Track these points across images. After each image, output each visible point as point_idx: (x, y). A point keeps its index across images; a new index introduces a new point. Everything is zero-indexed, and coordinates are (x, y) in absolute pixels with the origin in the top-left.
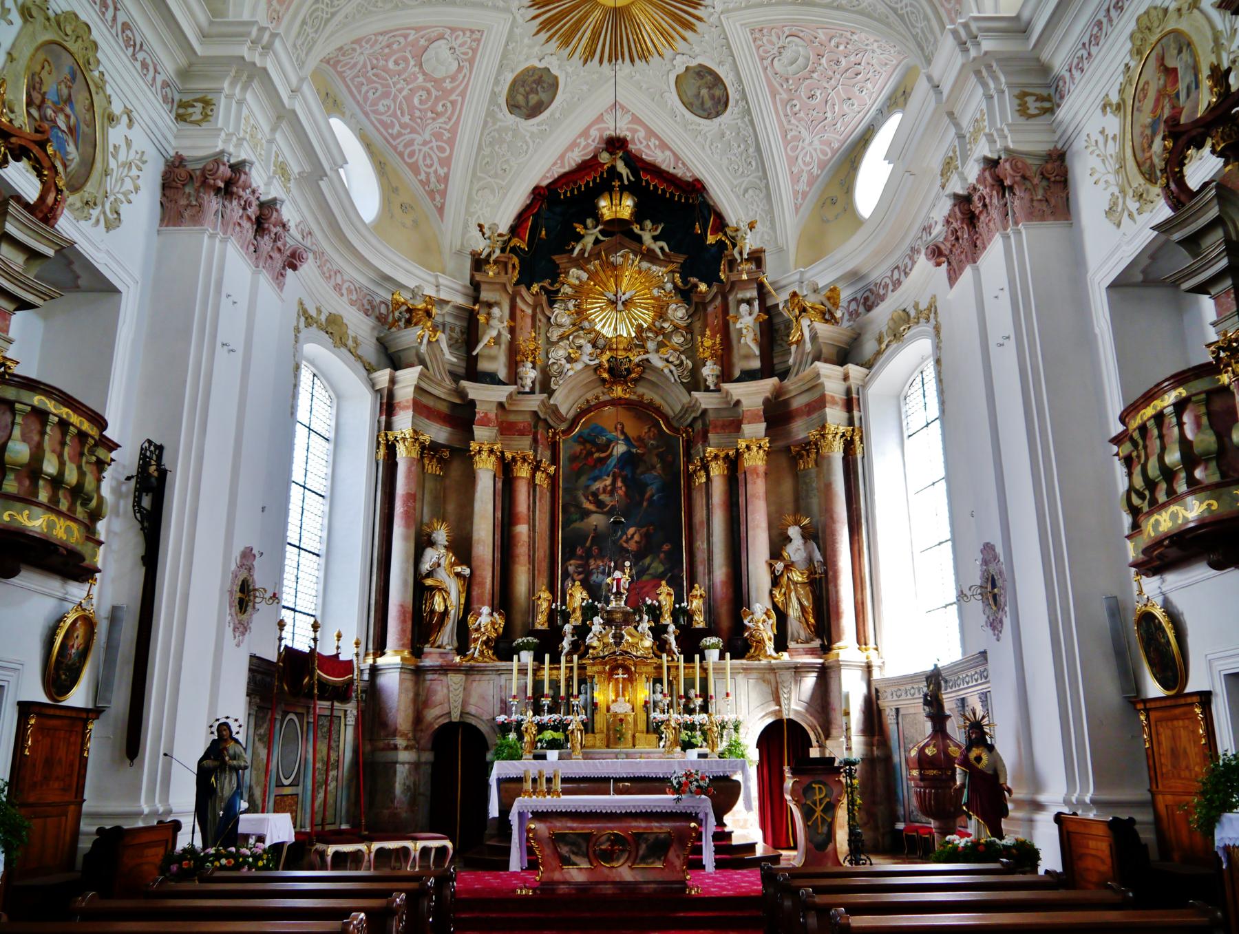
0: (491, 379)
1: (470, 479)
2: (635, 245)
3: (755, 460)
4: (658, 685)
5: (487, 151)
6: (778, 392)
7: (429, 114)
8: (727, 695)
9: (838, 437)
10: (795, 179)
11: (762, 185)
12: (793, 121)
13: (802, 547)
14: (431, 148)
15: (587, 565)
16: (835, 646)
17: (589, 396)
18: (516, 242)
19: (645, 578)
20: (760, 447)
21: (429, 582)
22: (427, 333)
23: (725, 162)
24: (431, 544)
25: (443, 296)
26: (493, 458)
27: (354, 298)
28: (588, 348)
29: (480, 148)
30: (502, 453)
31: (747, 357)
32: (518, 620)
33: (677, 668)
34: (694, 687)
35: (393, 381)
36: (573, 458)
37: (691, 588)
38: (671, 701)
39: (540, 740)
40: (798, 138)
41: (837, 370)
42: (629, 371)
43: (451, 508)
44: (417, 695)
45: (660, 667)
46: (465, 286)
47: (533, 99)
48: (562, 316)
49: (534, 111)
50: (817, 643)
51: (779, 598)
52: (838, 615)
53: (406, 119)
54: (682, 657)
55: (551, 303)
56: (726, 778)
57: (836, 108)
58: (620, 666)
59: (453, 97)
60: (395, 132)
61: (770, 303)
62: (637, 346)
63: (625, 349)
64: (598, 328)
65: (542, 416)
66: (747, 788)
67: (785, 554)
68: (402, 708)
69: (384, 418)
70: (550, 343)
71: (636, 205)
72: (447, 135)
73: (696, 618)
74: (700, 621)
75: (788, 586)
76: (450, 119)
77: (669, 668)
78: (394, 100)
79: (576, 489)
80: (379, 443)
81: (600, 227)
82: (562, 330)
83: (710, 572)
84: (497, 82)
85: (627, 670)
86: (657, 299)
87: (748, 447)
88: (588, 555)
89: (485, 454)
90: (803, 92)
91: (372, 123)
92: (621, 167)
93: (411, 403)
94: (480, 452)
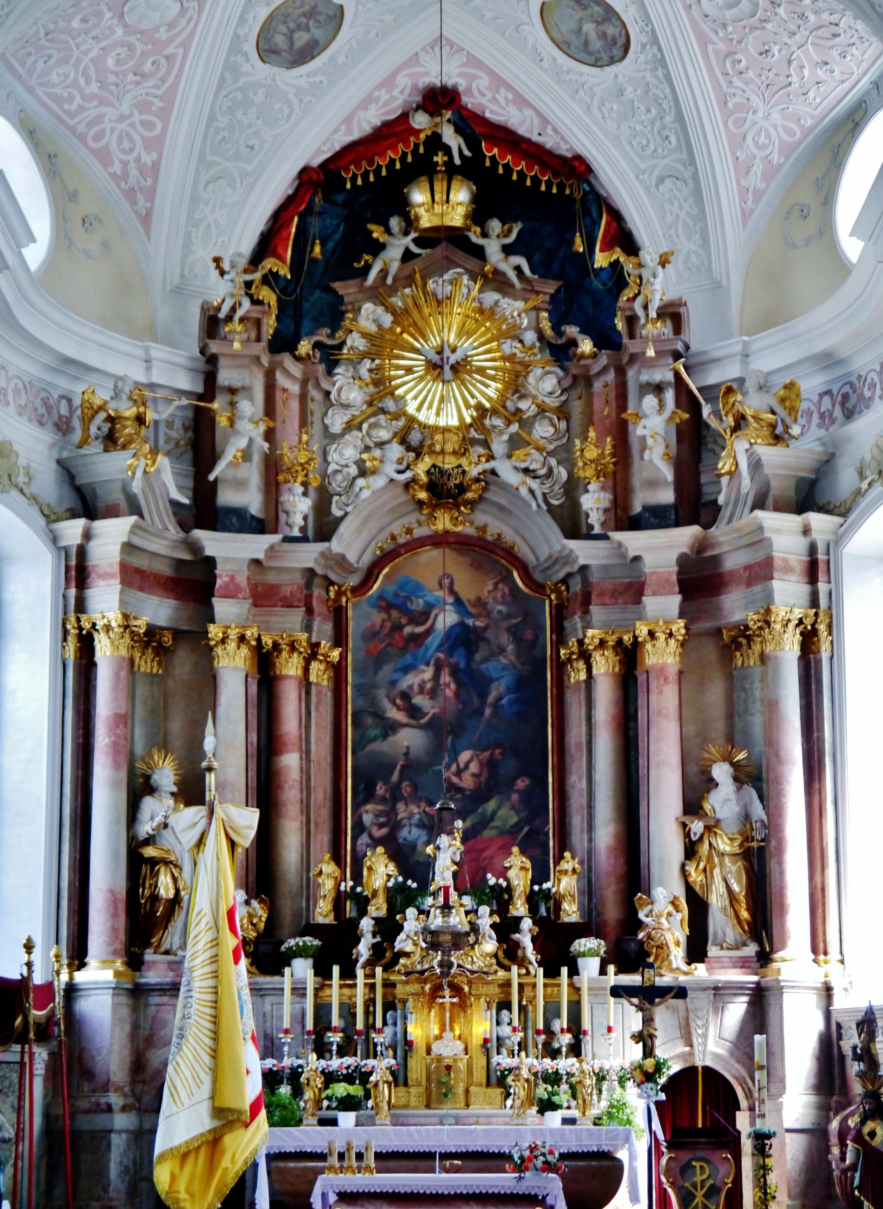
1: (208, 682)
2: (473, 263)
3: (662, 656)
4: (505, 1012)
5: (223, 121)
6: (701, 546)
7: (131, 77)
8: (610, 1029)
9: (791, 626)
10: (743, 169)
11: (688, 174)
12: (737, 82)
13: (733, 797)
14: (132, 125)
15: (393, 811)
16: (777, 956)
17: (396, 528)
19: (487, 833)
20: (671, 635)
21: (149, 852)
22: (143, 462)
24: (149, 789)
25: (156, 379)
26: (245, 651)
27: (23, 402)
28: (396, 450)
29: (212, 118)
30: (259, 639)
31: (653, 484)
32: (287, 907)
33: (534, 986)
34: (558, 1016)
35: (87, 535)
36: (371, 635)
37: (559, 858)
38: (526, 1037)
39: (329, 1098)
40: (746, 107)
41: (793, 521)
42: (462, 488)
43: (176, 726)
44: (136, 1027)
45: (507, 984)
46: (192, 359)
47: (301, 39)
48: (349, 389)
49: (304, 55)
50: (751, 949)
51: (696, 877)
53: (94, 88)
54: (541, 971)
56: (606, 1156)
57: (806, 72)
58: (448, 989)
59: (170, 50)
60: (74, 106)
62: (474, 442)
63: (454, 453)
64: (411, 409)
65: (319, 571)
66: (633, 1170)
67: (707, 807)
68: (116, 1048)
69: (72, 592)
70: (331, 437)
71: (476, 199)
72: (158, 103)
73: (565, 906)
74: (571, 913)
75: (710, 858)
76: (163, 80)
77: (521, 986)
78: (76, 66)
79: (375, 687)
80: (65, 632)
81: (413, 235)
83: (591, 828)
84: (242, 21)
85: (456, 990)
86: (511, 358)
87: (652, 634)
88: (395, 796)
89: (232, 646)
90: (752, 44)
91: (39, 100)
92: (451, 138)
93: (116, 568)
94: (223, 641)
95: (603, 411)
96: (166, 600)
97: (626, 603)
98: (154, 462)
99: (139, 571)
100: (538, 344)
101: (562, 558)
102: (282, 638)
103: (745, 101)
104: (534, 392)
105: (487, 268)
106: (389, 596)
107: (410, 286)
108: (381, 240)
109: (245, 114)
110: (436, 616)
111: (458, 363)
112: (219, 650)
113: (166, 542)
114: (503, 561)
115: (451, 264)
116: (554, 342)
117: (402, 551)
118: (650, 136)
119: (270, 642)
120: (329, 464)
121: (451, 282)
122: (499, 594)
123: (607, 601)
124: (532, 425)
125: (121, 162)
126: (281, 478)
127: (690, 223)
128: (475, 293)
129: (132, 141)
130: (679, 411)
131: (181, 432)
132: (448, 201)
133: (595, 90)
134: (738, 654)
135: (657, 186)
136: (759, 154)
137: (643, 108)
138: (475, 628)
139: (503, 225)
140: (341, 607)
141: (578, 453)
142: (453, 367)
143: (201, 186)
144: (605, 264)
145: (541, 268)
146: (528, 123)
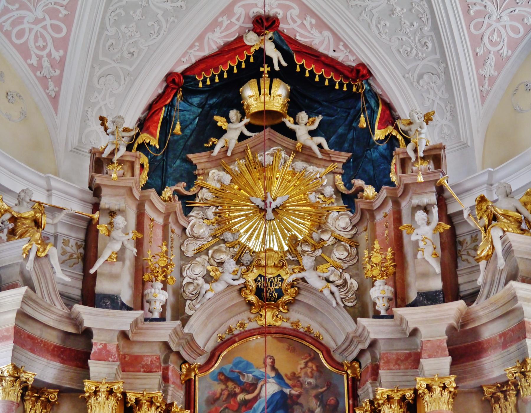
0: (113, 302)
2: (288, 142)
5: (111, 31)
6: (465, 320)
10: (480, 61)
11: (440, 69)
14: (44, 27)
17: (233, 323)
18: (144, 137)
20: (444, 388)
22: (35, 247)
25: (55, 202)
26: (112, 401)
28: (231, 265)
29: (103, 28)
30: (124, 394)
31: (425, 275)
36: (213, 400)
40: (484, 13)
42: (281, 293)
46: (82, 191)
48: (200, 225)
55: (187, 210)
61: (452, 209)
62: (290, 262)
63: (275, 266)
64: (243, 240)
65: (174, 348)
71: (291, 95)
72: (64, 12)
81: (246, 120)
82: (199, 243)
86: (314, 206)
87: (429, 388)
89: (102, 396)
93: (12, 333)
94: (96, 393)
95: (384, 234)
96: (52, 363)
97: (407, 369)
98: (44, 250)
99: (31, 338)
100: (334, 196)
101: (357, 337)
102: (143, 396)
103: (483, 8)
104: (333, 228)
105: (298, 144)
106: (227, 373)
107: (244, 158)
108: (224, 128)
109: (127, 27)
110: (262, 386)
111: (277, 208)
112: (92, 401)
113: (54, 317)
114: (311, 346)
115: (274, 143)
116: (346, 193)
117: (237, 339)
118: (413, 44)
119: (133, 399)
120: (184, 278)
121: (272, 155)
122: (309, 370)
123: (392, 367)
124: (331, 251)
125: (37, 56)
126: (146, 277)
127: (443, 105)
128: (289, 162)
129: (45, 40)
130: (443, 224)
131: (75, 248)
132: (270, 94)
133: (374, 11)
134: (497, 406)
135: (418, 82)
136: (493, 49)
137: (408, 23)
138: (291, 396)
139: (309, 117)
140: (190, 380)
141: (367, 259)
142: (273, 210)
143: (95, 79)
144: (382, 138)
145: (337, 146)
146: (326, 42)
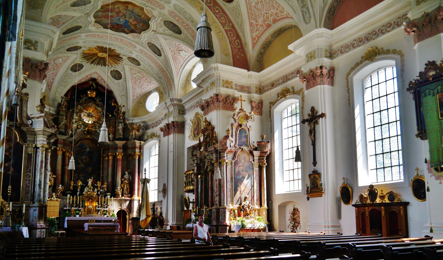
3: (120, 157)
5: (63, 78)
6: (125, 143)
10: (134, 96)
17: (81, 136)
23: (118, 89)
25: (51, 112)
28: (83, 126)
40: (136, 89)
41: (139, 142)
50: (129, 195)
51: (122, 186)
52: (134, 190)
64: (85, 120)
70: (73, 123)
71: (96, 94)
84: (70, 65)
87: (119, 154)
90: (139, 81)
92: (94, 85)
